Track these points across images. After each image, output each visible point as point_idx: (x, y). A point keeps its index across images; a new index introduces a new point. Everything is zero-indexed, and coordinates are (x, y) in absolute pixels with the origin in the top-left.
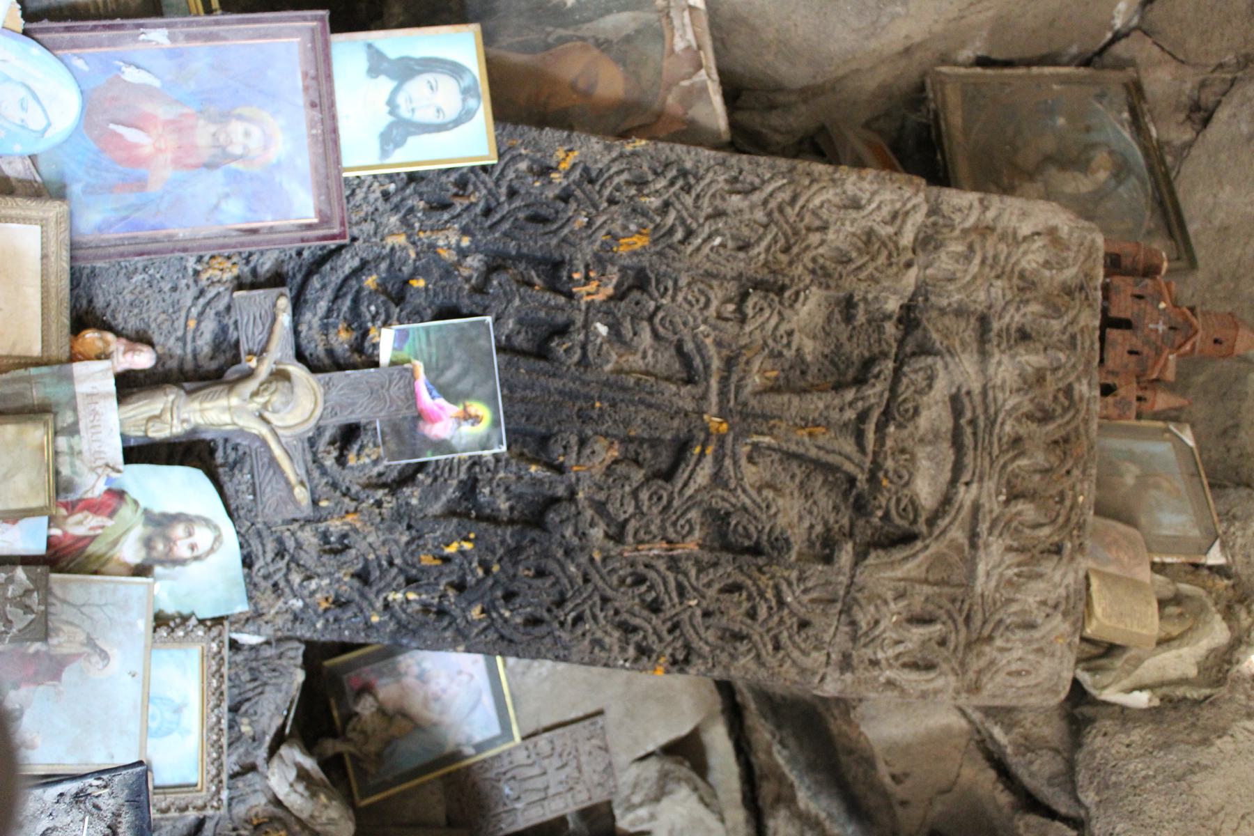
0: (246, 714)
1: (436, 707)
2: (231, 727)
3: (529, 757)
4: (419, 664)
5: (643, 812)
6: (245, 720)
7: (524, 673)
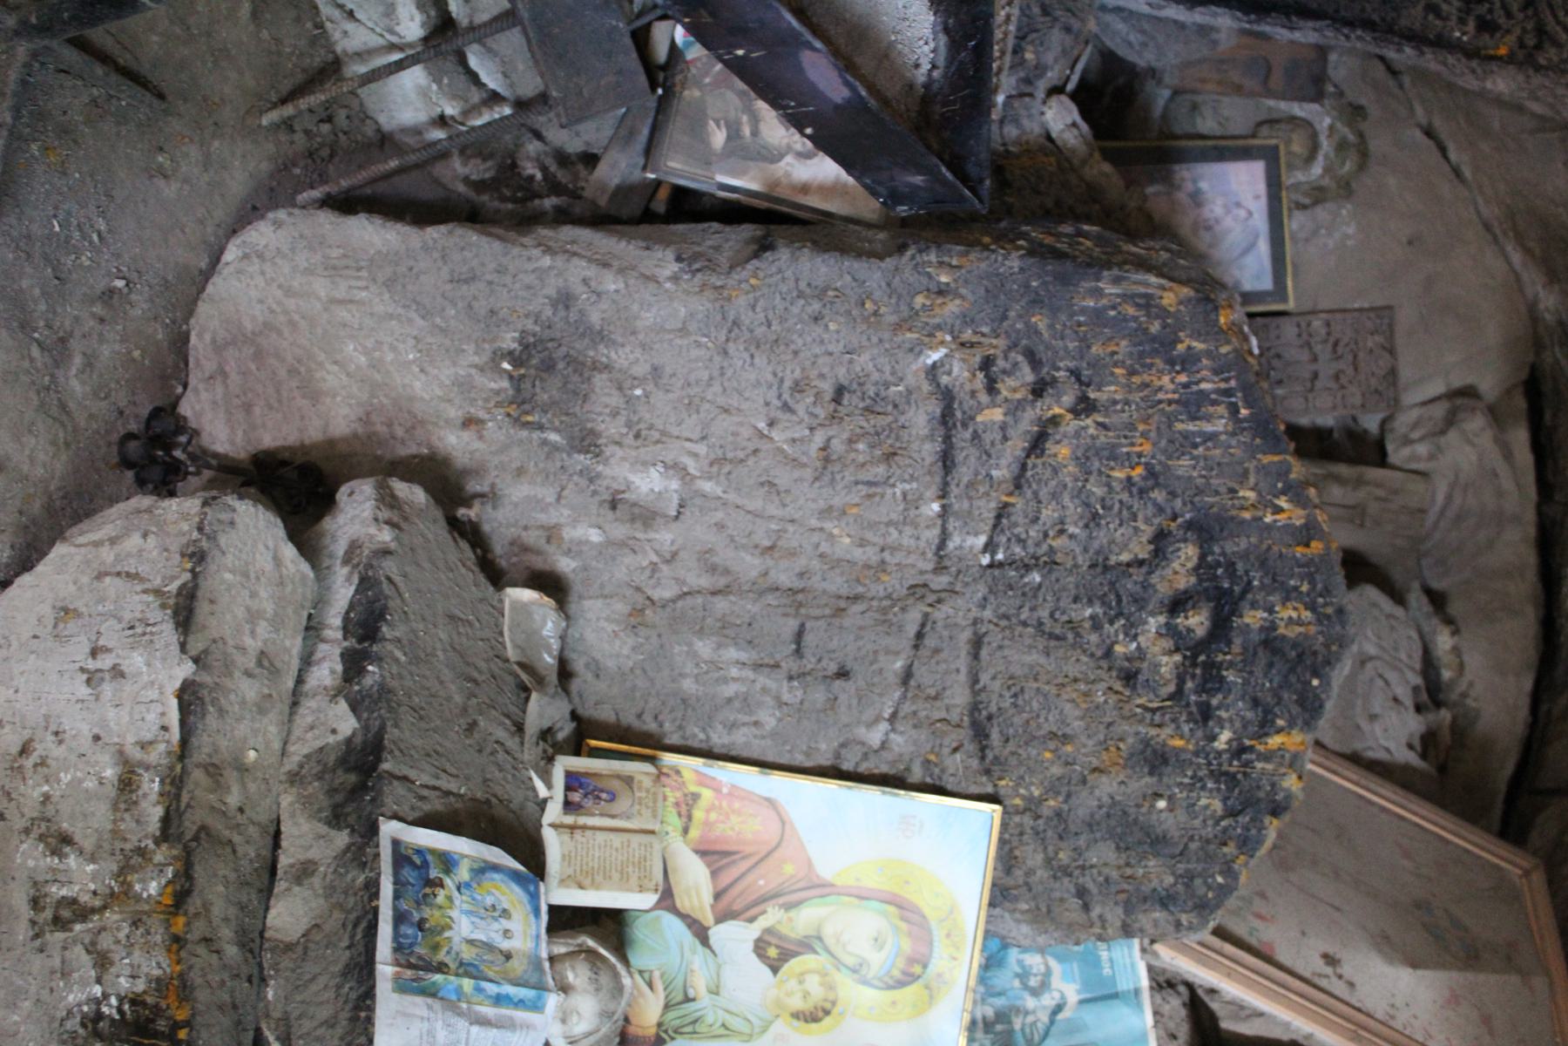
0: (1032, 42)
1: (1206, 237)
2: (1015, 52)
3: (1299, 335)
4: (1195, 181)
5: (1422, 449)
6: (1030, 48)
7: (1307, 240)
